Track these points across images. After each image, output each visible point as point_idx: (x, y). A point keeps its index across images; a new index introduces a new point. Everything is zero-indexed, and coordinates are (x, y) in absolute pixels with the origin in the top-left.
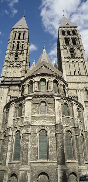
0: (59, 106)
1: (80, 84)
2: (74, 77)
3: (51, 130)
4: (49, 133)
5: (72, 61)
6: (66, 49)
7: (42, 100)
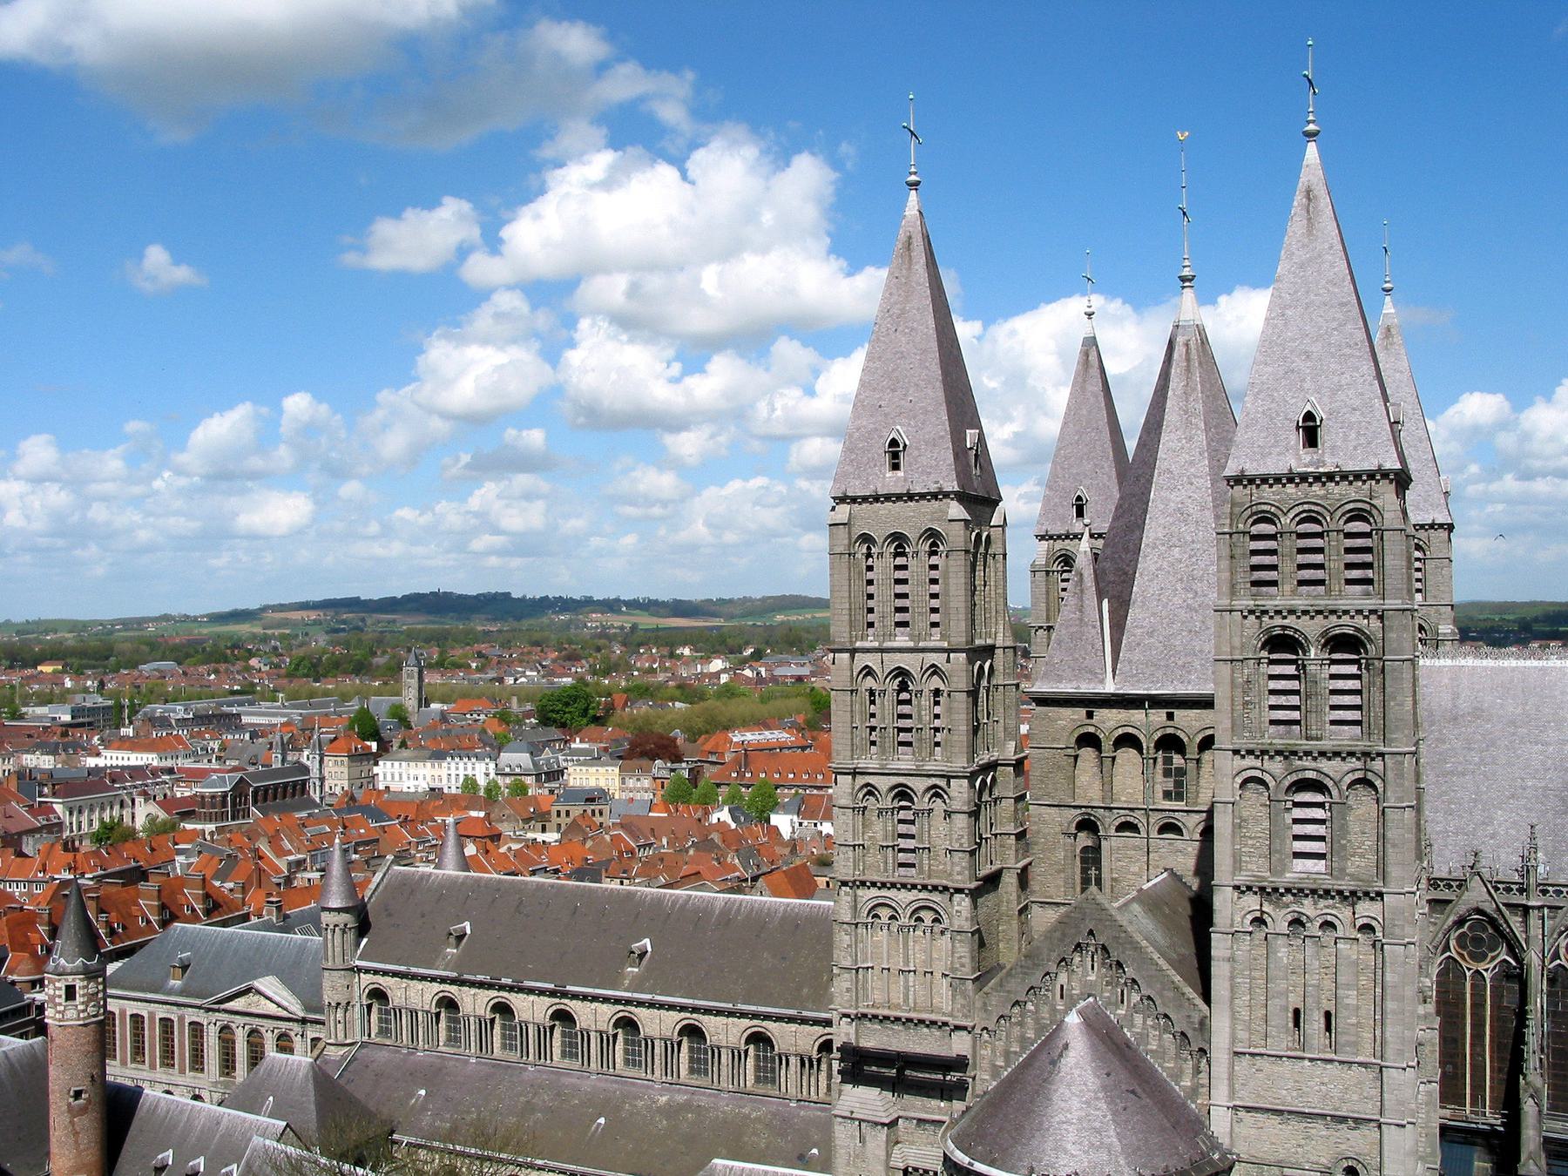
1: (1318, 1129)
5: (1291, 923)
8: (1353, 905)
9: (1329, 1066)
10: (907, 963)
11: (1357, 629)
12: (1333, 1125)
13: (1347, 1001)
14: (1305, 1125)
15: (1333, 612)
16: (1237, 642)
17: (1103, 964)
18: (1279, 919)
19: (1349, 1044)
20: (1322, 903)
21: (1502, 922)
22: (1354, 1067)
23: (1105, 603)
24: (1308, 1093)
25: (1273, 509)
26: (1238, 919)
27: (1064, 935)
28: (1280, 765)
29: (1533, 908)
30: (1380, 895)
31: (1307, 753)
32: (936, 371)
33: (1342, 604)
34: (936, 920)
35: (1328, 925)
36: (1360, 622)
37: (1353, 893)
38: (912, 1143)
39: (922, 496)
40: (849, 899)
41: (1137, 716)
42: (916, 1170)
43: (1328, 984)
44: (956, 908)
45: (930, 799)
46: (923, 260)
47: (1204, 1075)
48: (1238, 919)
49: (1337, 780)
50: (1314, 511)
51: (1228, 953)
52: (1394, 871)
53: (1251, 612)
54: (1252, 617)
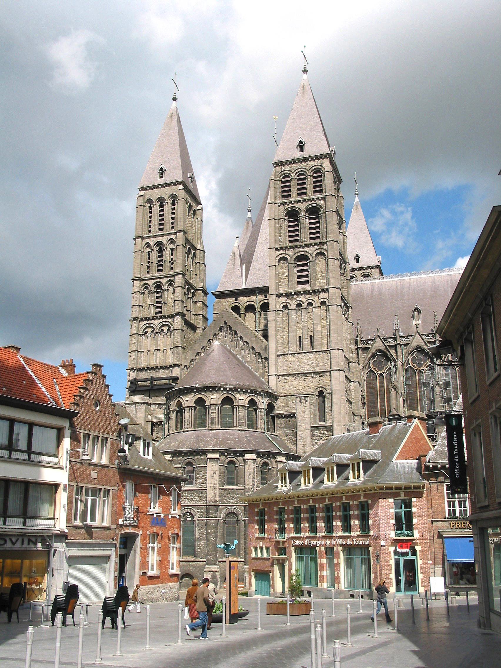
0: (215, 472)
1: (309, 378)
3: (200, 513)
4: (196, 518)
6: (285, 259)
7: (187, 461)
9: (312, 354)
10: (157, 347)
11: (317, 204)
13: (317, 329)
15: (309, 200)
16: (276, 214)
17: (230, 334)
18: (293, 305)
19: (318, 345)
20: (308, 296)
21: (388, 353)
22: (321, 353)
23: (244, 267)
24: (305, 365)
25: (289, 172)
26: (278, 306)
27: (215, 324)
28: (292, 252)
29: (399, 344)
30: (327, 290)
31: (301, 246)
32: (178, 154)
34: (168, 330)
35: (310, 304)
36: (318, 202)
37: (318, 290)
38: (156, 414)
40: (136, 325)
42: (157, 423)
43: (311, 326)
45: (168, 286)
46: (176, 119)
47: (267, 368)
48: (278, 306)
49: (311, 253)
51: (274, 318)
52: (332, 281)
53: (281, 204)
54: (282, 206)
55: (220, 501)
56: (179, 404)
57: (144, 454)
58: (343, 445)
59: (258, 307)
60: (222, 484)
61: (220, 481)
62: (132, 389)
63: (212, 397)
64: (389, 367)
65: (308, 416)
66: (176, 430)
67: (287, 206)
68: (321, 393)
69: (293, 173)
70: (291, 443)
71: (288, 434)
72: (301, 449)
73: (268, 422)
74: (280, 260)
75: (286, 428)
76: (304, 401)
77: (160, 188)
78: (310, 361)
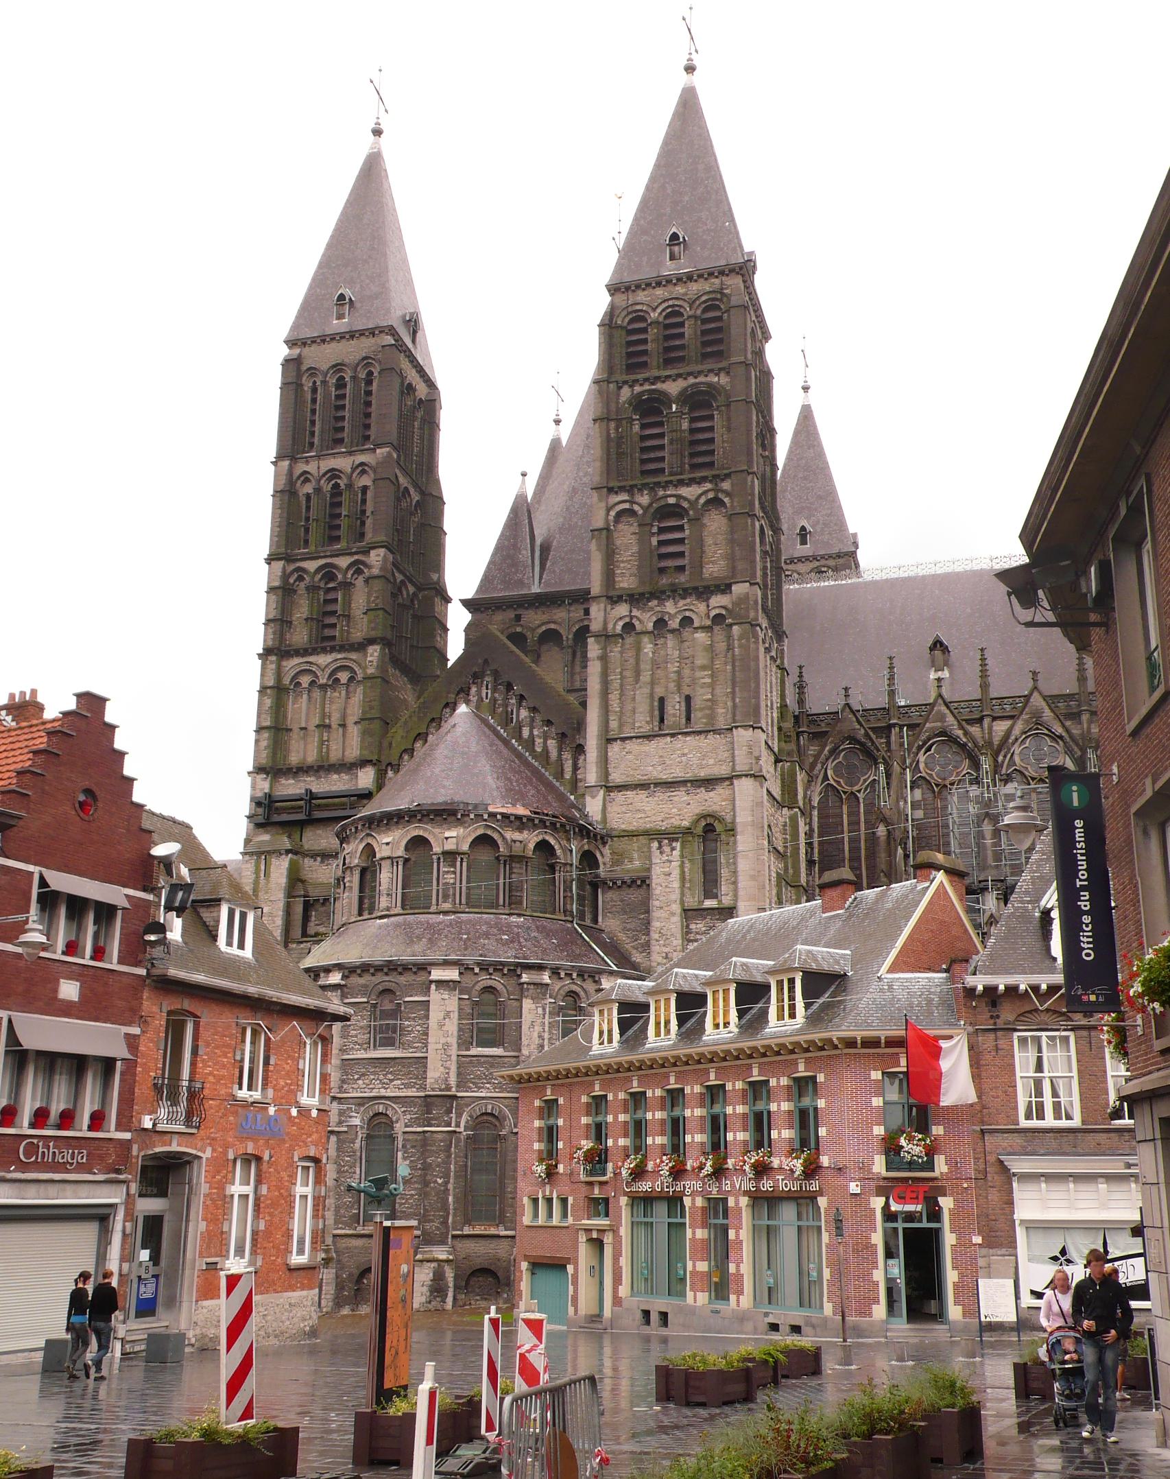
0: (448, 1014)
1: (681, 796)
2: (652, 747)
3: (408, 1117)
4: (399, 1128)
6: (631, 512)
8: (708, 599)
9: (688, 739)
11: (710, 385)
12: (692, 790)
14: (669, 794)
18: (646, 620)
20: (682, 603)
22: (710, 736)
24: (671, 765)
29: (894, 725)
33: (700, 367)
39: (362, 333)
40: (273, 666)
41: (560, 614)
44: (369, 659)
45: (352, 575)
48: (610, 626)
50: (677, 306)
53: (625, 382)
55: (461, 1085)
56: (369, 851)
57: (229, 944)
58: (754, 940)
59: (567, 635)
60: (464, 1043)
61: (459, 1037)
62: (261, 820)
63: (447, 834)
64: (871, 779)
65: (676, 885)
66: (360, 914)
67: (637, 389)
68: (709, 829)
69: (654, 310)
70: (633, 947)
71: (628, 926)
72: (659, 964)
73: (581, 898)
74: (619, 515)
75: (625, 913)
76: (667, 849)
77: (338, 341)
78: (684, 755)
